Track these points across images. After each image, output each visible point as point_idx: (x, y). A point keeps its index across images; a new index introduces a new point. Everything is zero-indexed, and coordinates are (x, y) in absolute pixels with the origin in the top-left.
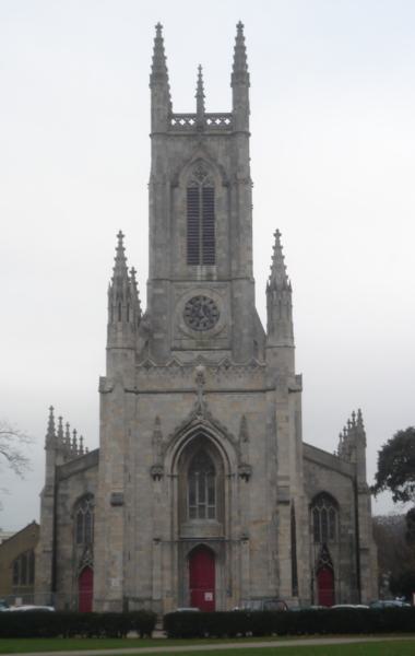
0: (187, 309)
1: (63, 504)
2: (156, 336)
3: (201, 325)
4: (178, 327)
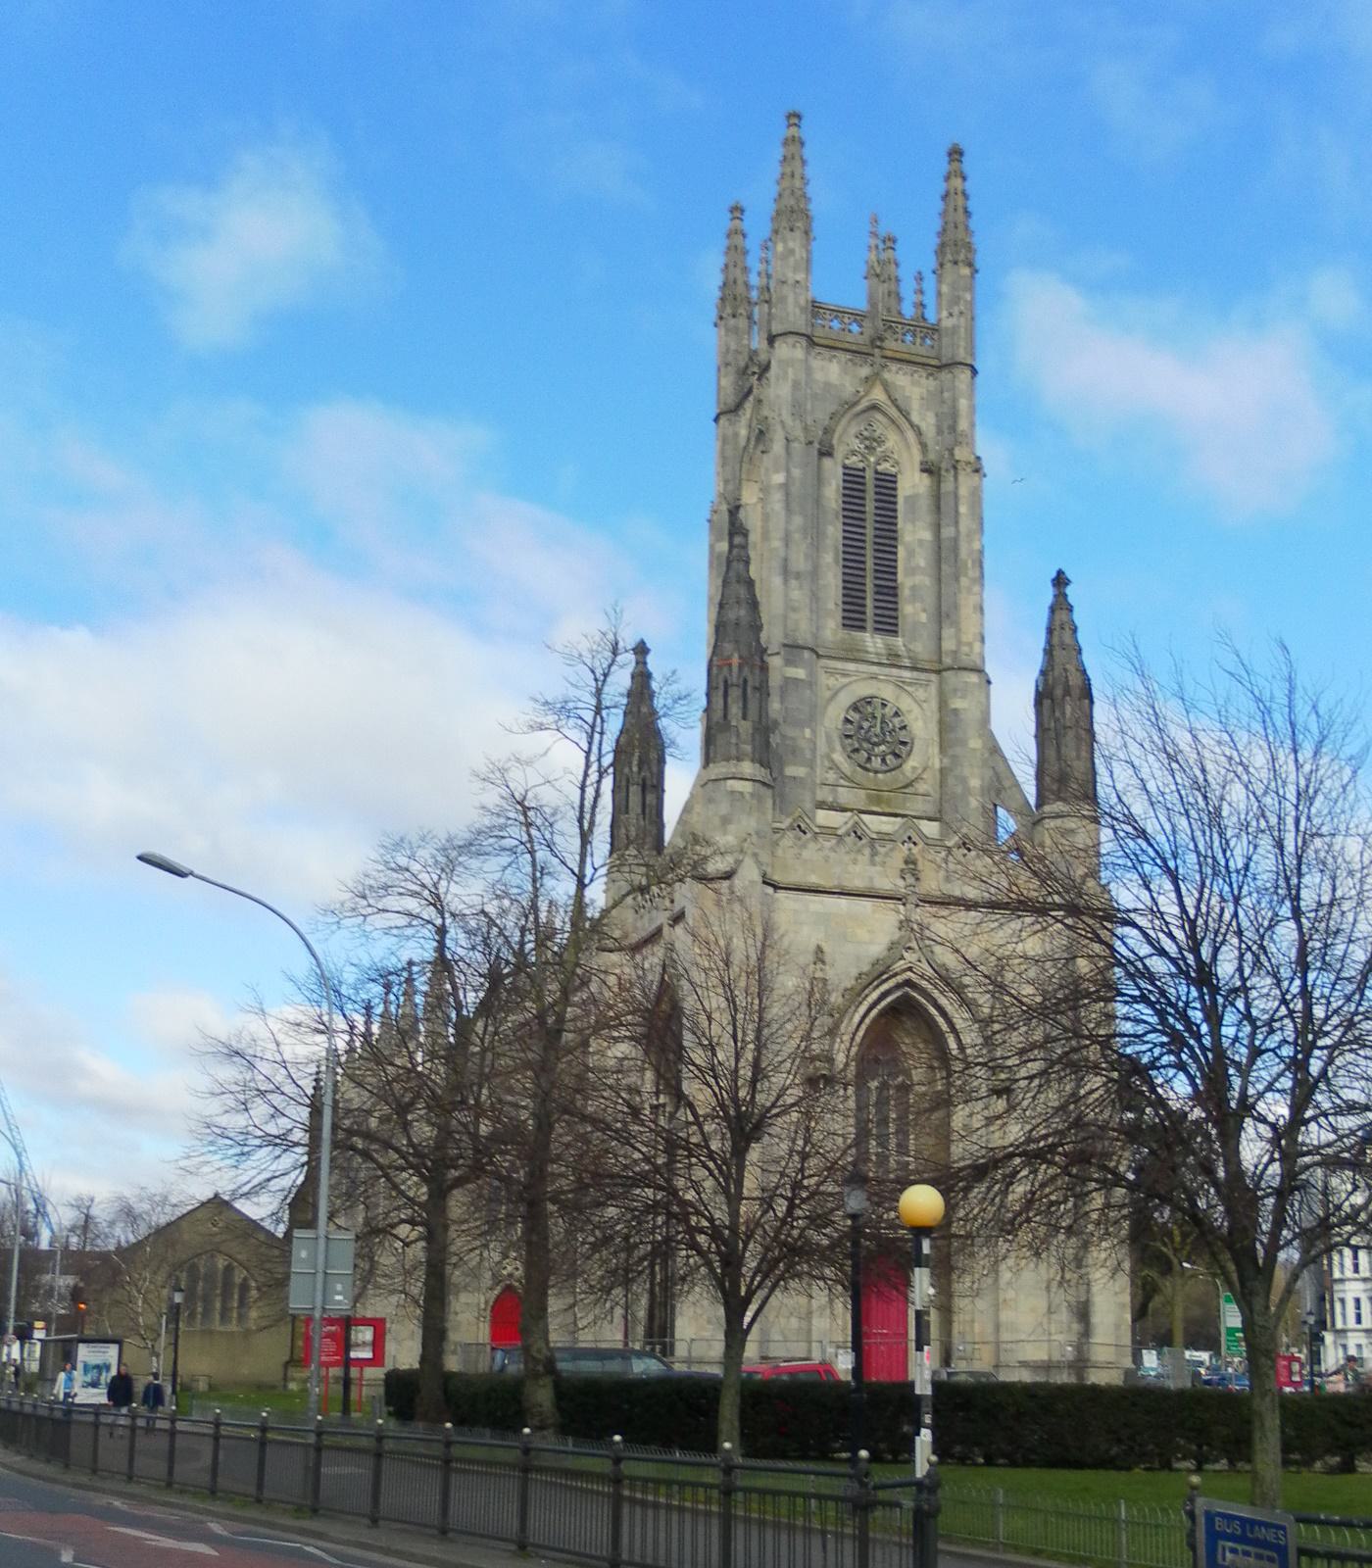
0: (847, 721)
2: (791, 771)
3: (876, 763)
4: (828, 757)
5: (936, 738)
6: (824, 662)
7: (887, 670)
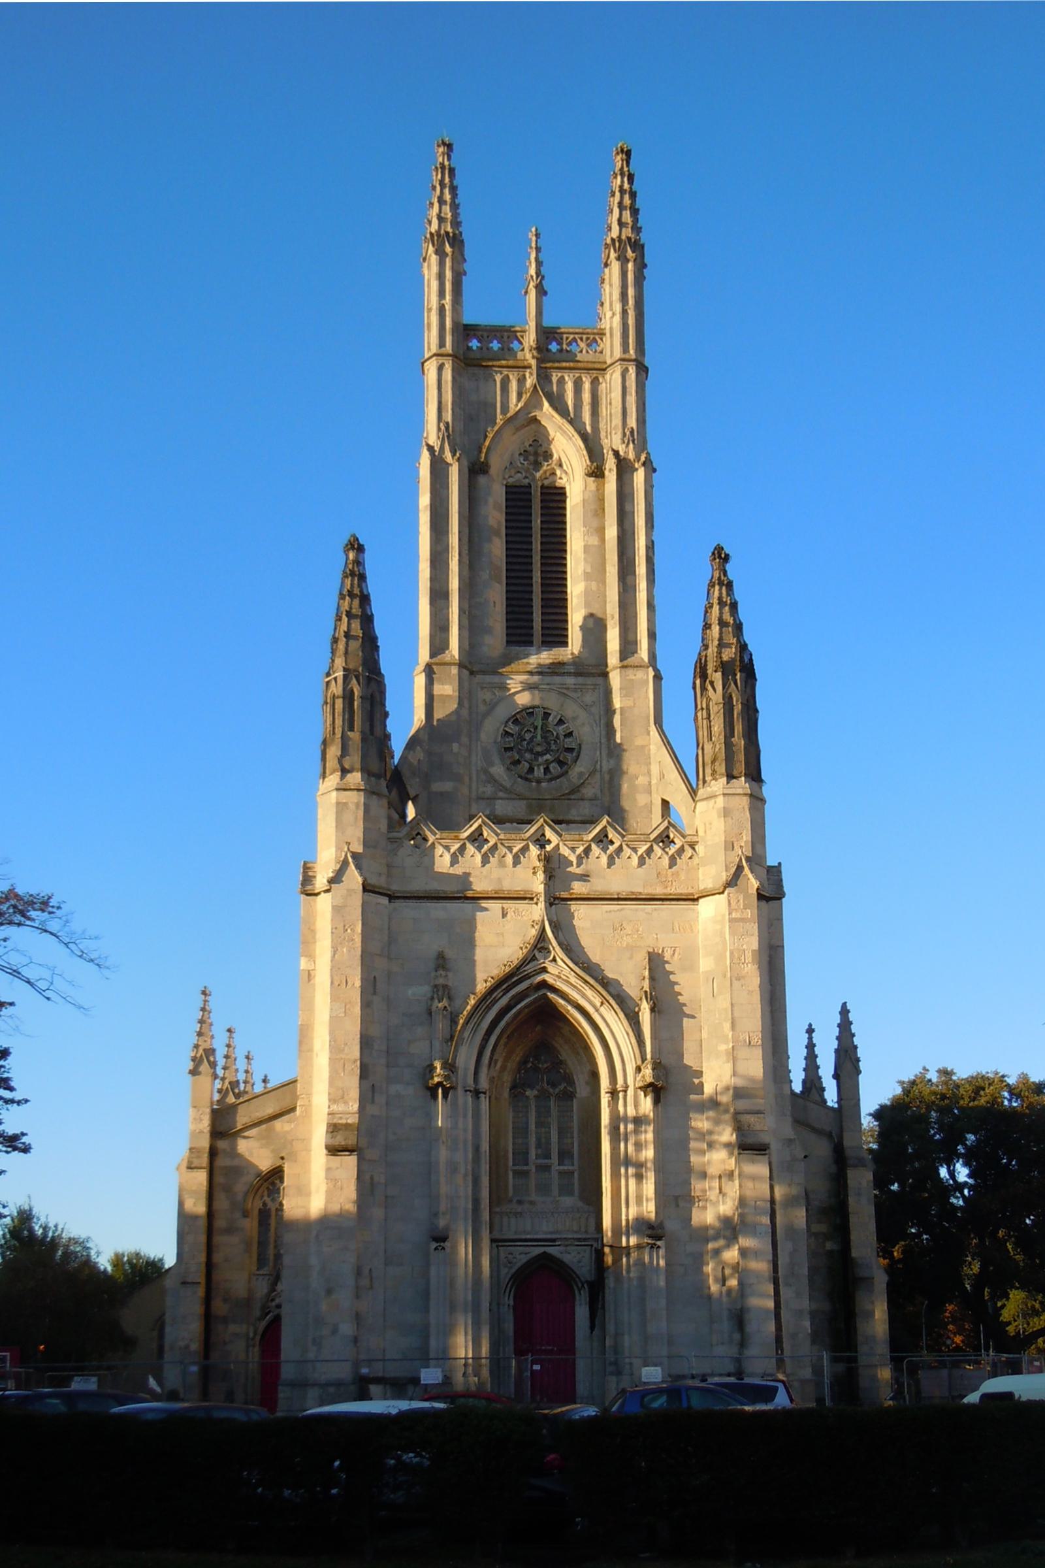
1: (227, 1189)
2: (437, 787)
3: (539, 772)
4: (486, 772)
5: (603, 740)
6: (479, 678)
7: (548, 679)
